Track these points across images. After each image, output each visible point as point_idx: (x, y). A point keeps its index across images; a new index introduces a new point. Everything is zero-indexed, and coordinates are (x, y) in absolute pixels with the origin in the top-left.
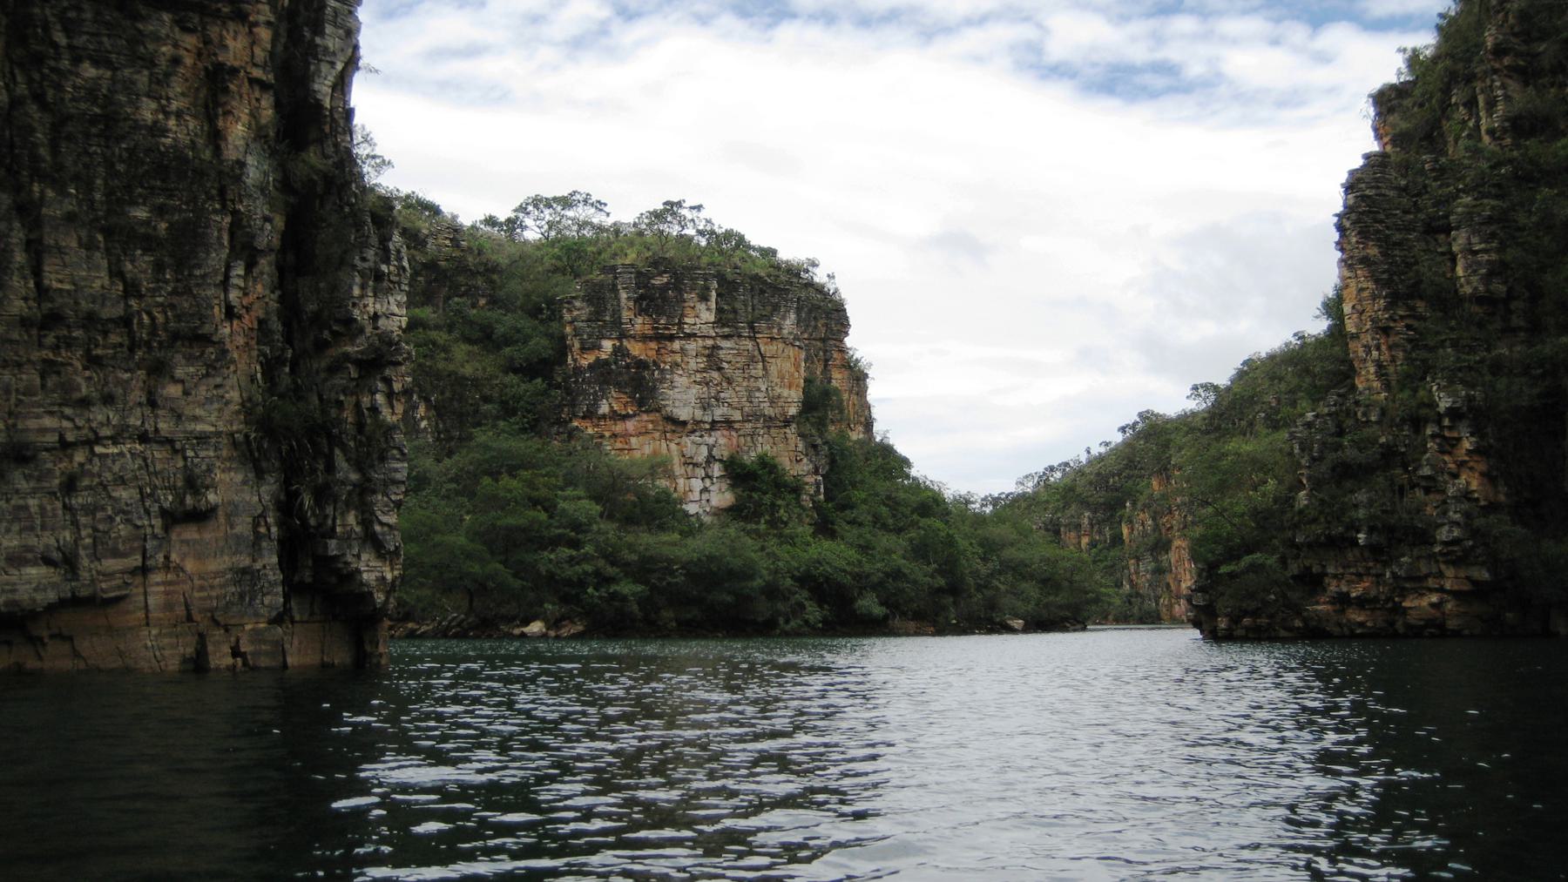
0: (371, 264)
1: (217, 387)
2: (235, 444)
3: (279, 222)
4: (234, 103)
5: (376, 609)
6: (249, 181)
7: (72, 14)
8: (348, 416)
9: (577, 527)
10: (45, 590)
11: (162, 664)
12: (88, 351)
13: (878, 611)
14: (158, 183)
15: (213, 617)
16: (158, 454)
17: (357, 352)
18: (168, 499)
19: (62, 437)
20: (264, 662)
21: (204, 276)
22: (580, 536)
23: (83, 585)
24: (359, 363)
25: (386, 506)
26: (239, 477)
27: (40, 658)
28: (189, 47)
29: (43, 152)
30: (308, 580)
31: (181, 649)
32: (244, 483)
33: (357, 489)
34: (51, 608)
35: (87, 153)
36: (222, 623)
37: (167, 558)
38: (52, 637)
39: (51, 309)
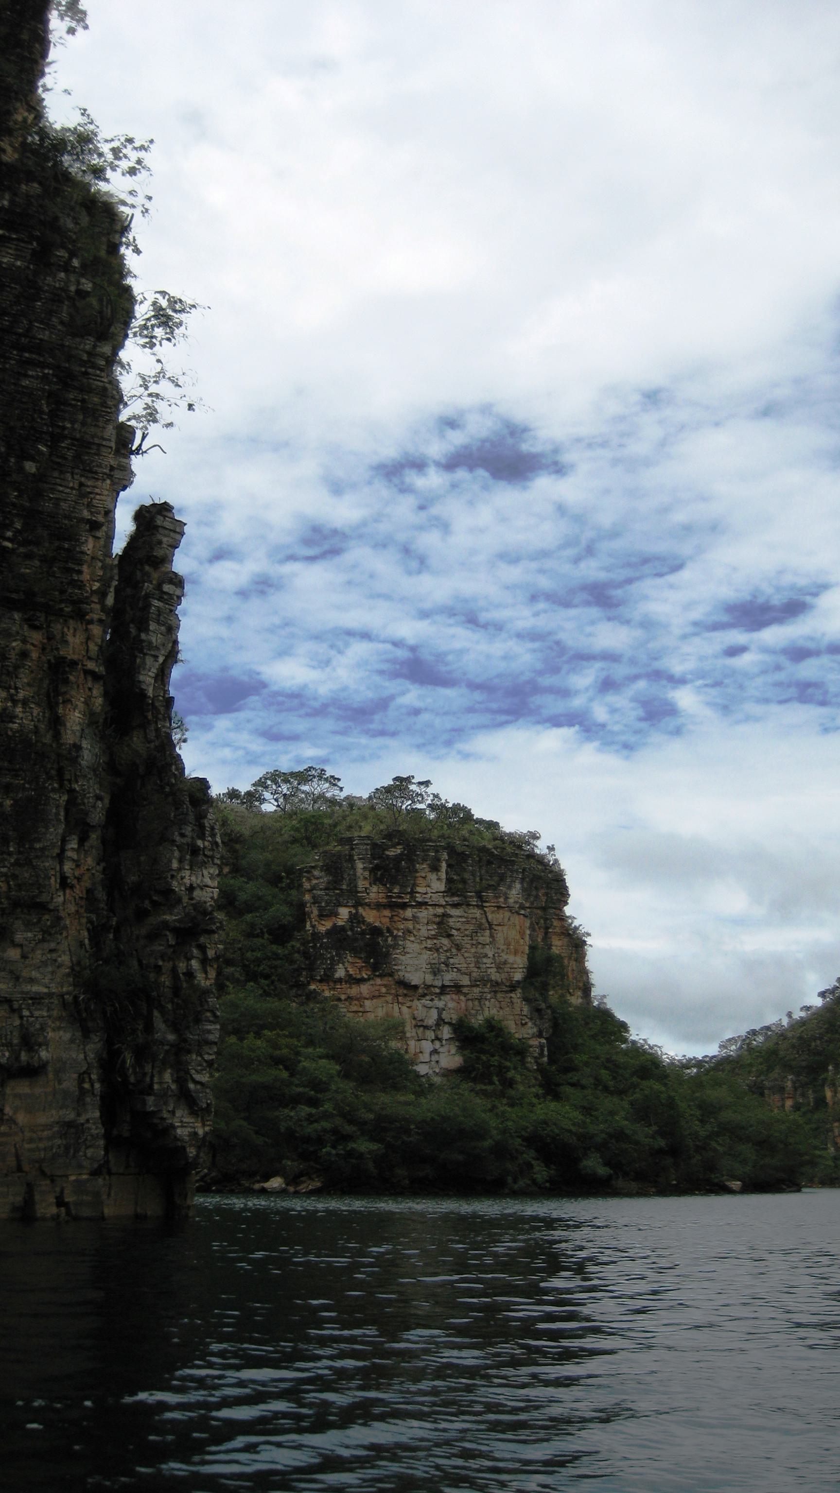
0: (189, 840)
1: (51, 951)
2: (64, 1005)
3: (107, 801)
4: (73, 693)
6: (84, 763)
8: (166, 980)
9: (318, 1085)
13: (603, 1171)
14: (6, 764)
17: (175, 921)
20: (86, 1212)
21: (43, 849)
22: (319, 1096)
24: (176, 931)
25: (201, 1065)
26: (67, 1036)
28: (35, 643)
32: (72, 1041)
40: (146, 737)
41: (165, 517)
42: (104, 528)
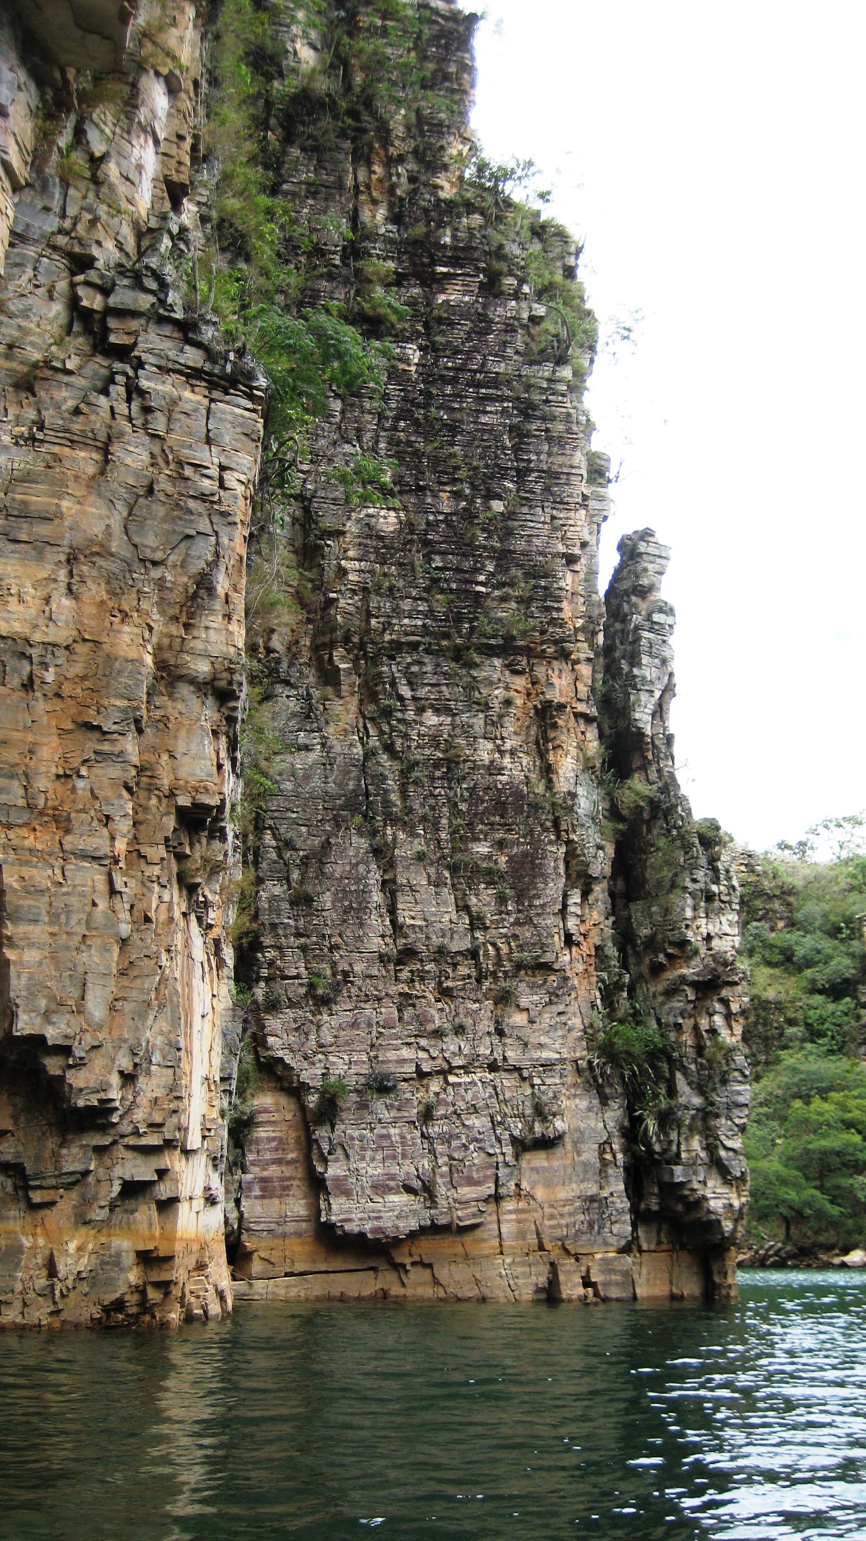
2: (579, 1071)
3: (610, 850)
4: (563, 738)
5: (724, 1238)
7: (415, 669)
8: (688, 1038)
10: (407, 1217)
11: (516, 1293)
12: (440, 983)
14: (497, 818)
15: (563, 1245)
16: (507, 1081)
17: (693, 974)
18: (518, 1128)
19: (418, 1066)
20: (614, 1293)
21: (543, 906)
23: (442, 1213)
24: (695, 985)
25: (731, 1130)
26: (584, 1104)
27: (403, 1285)
28: (519, 689)
29: (394, 797)
30: (655, 1208)
31: (534, 1278)
32: (590, 1109)
33: (700, 1114)
34: (412, 1235)
35: (432, 795)
36: (573, 1252)
37: (518, 1185)
38: (414, 1264)
39: (405, 944)
40: (648, 780)
41: (648, 542)
42: (583, 561)
